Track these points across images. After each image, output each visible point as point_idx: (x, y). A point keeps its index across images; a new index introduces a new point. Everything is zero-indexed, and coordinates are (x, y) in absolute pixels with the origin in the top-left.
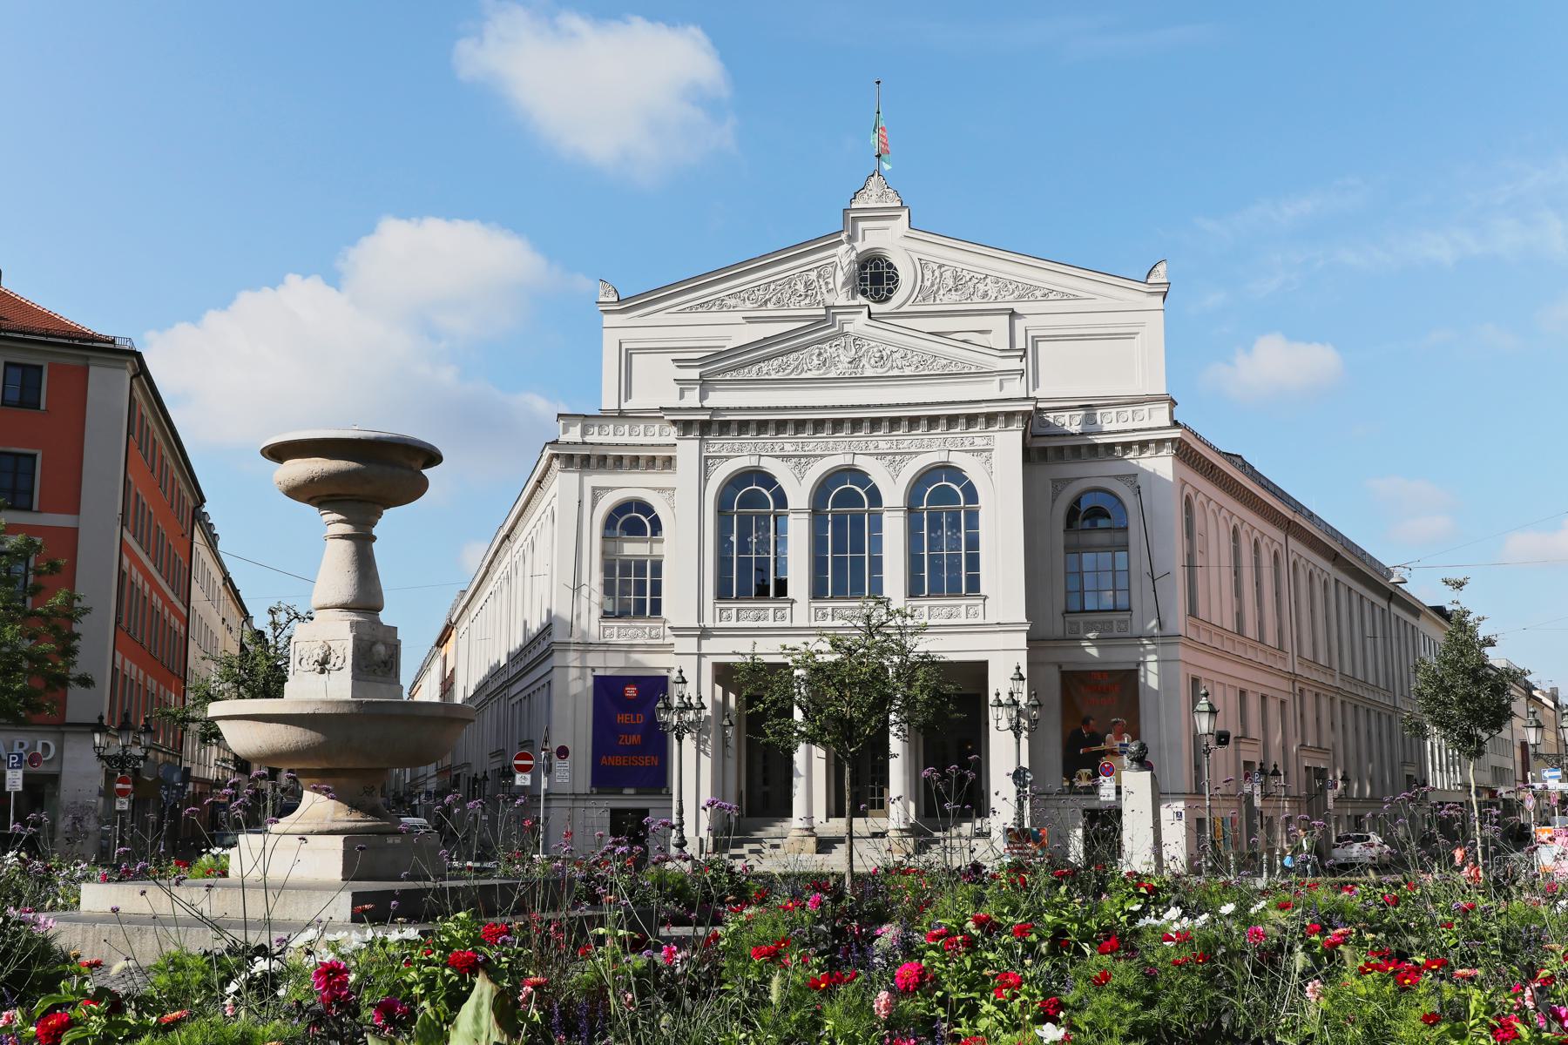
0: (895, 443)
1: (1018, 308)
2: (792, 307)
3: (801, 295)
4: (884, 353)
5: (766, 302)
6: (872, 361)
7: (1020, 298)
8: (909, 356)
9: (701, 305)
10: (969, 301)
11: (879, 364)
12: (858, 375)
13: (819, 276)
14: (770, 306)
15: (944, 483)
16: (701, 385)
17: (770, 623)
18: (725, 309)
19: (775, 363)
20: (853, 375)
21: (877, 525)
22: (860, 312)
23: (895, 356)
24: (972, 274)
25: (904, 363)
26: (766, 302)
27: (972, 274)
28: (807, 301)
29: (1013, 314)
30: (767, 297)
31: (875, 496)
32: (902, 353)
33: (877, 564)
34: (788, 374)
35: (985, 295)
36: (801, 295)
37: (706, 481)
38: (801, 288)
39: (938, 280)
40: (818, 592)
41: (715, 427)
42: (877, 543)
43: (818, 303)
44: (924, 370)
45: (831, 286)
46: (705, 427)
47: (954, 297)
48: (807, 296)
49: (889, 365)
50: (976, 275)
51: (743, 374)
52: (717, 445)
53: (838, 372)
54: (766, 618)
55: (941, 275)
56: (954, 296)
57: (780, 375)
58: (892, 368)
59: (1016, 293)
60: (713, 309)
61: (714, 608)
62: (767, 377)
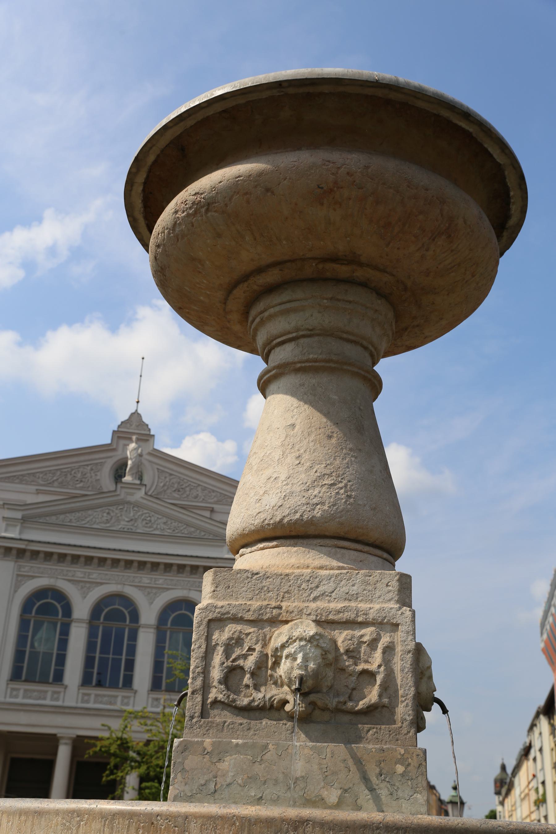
0: (153, 580)
1: (215, 506)
2: (70, 487)
3: (77, 481)
4: (153, 519)
5: (53, 482)
6: (144, 522)
7: (216, 503)
8: (169, 522)
9: (9, 477)
10: (186, 499)
11: (149, 525)
12: (133, 531)
13: (92, 469)
14: (56, 484)
15: (183, 612)
16: (22, 523)
17: (48, 702)
18: (24, 482)
19: (78, 514)
20: (130, 530)
21: (134, 636)
22: (140, 489)
23: (159, 521)
24: (189, 483)
25: (165, 527)
26: (53, 482)
27: (189, 483)
28: (81, 485)
29: (212, 511)
30: (55, 478)
31: (135, 616)
32: (164, 520)
33: (130, 665)
34: (85, 524)
35: (196, 497)
36: (77, 481)
37: (15, 591)
38: (79, 475)
39: (168, 483)
40: (86, 681)
41: (28, 554)
42: (132, 650)
43: (88, 487)
44: (178, 533)
45: (98, 478)
46: (21, 553)
47: (176, 496)
48: (81, 481)
49: (155, 526)
50: (192, 484)
51: (53, 519)
52: (28, 566)
53: (120, 527)
54: (45, 699)
55: (170, 480)
56: (176, 495)
57: (78, 524)
58: (156, 529)
59: (215, 499)
60: (16, 481)
61: (7, 688)
62: (69, 524)
